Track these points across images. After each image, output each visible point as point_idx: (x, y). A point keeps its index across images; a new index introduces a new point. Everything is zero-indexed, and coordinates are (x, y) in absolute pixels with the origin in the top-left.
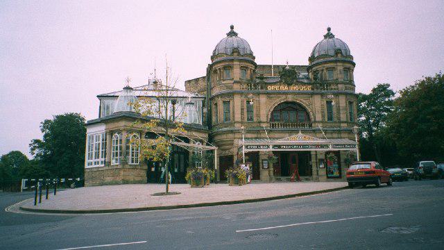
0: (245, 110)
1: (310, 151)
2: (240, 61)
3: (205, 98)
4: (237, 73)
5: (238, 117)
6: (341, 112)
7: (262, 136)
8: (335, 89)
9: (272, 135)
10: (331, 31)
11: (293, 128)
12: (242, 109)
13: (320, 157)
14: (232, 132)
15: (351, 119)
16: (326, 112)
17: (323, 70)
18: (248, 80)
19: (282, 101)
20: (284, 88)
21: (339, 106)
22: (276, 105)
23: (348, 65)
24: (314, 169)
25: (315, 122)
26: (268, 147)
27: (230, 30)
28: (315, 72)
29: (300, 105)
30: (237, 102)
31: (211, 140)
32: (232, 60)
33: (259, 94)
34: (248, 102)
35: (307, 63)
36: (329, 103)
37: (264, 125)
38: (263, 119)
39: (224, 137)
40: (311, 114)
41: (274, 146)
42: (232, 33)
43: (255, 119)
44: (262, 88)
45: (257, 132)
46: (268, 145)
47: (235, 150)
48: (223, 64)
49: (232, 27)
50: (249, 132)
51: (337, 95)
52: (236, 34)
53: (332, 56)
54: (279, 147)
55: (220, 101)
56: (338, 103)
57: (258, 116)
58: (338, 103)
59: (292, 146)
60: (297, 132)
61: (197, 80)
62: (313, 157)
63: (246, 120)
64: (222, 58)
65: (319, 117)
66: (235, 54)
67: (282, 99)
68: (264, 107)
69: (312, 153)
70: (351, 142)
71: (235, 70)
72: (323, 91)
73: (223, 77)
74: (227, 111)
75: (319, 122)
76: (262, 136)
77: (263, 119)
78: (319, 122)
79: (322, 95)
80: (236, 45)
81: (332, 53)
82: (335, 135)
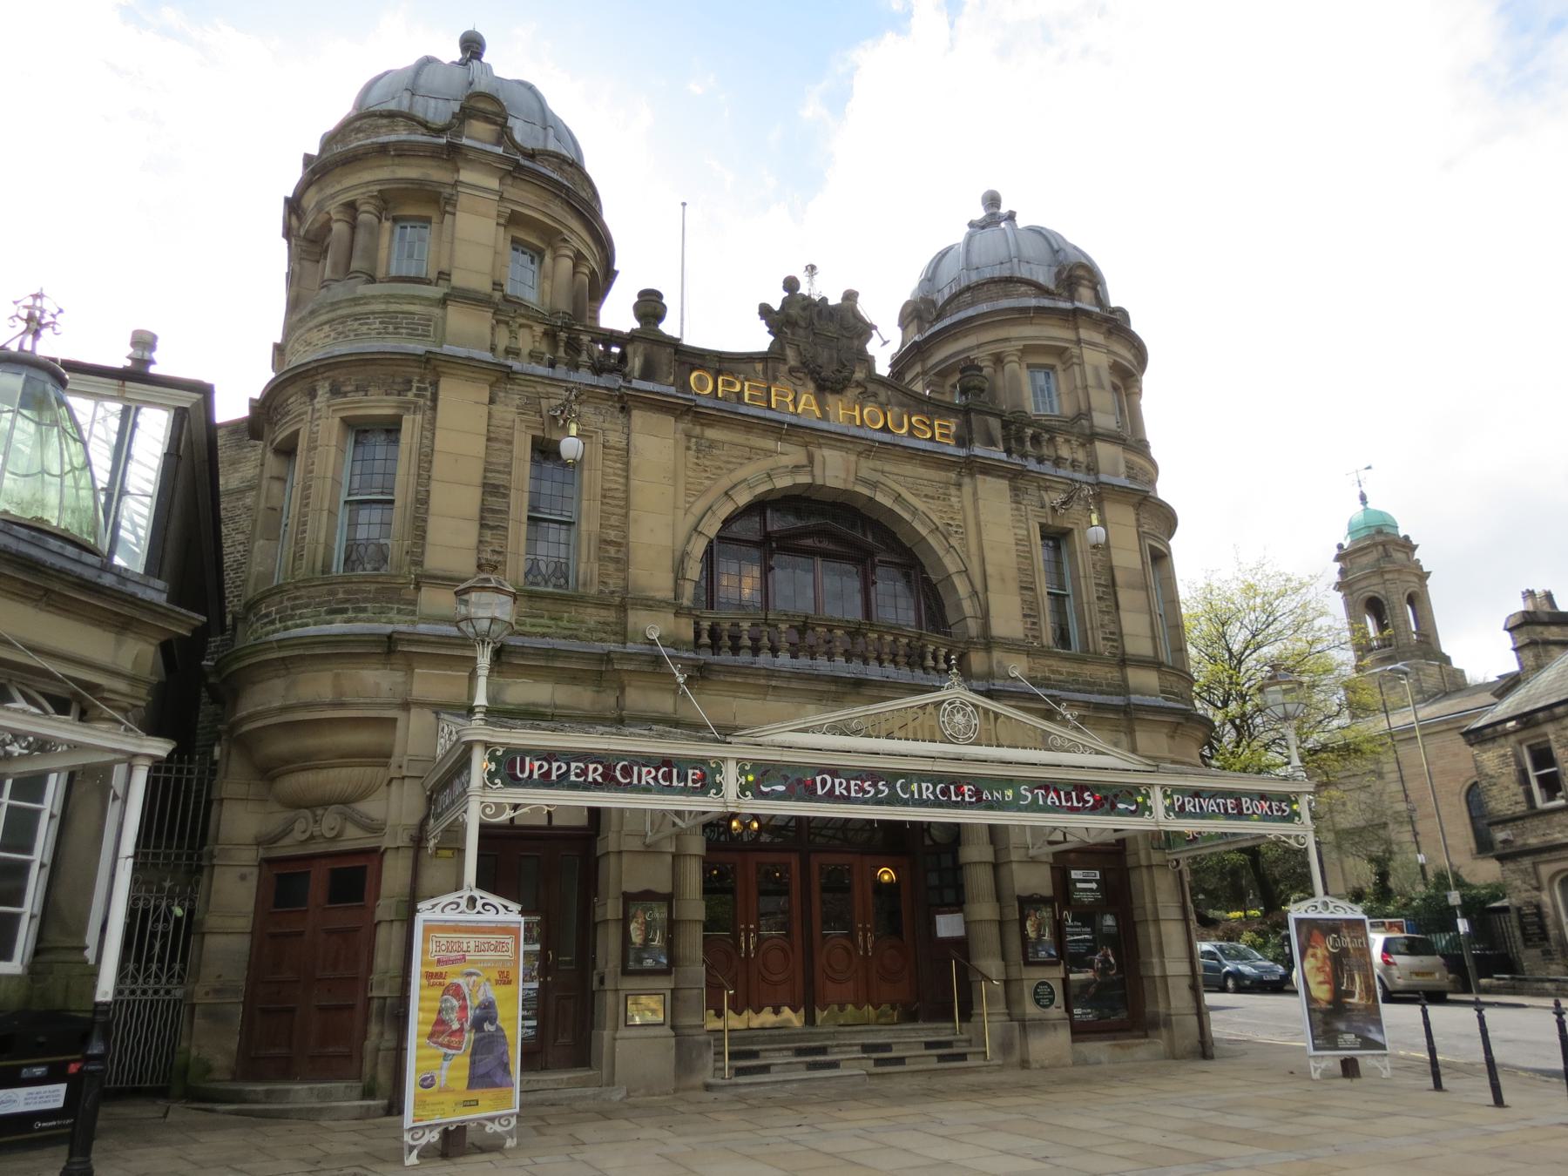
4: (474, 240)
6: (1124, 597)
8: (1074, 464)
10: (1004, 210)
11: (855, 669)
12: (492, 490)
16: (1043, 587)
17: (998, 360)
19: (783, 482)
21: (1111, 569)
22: (743, 498)
25: (988, 642)
26: (707, 784)
30: (462, 421)
33: (625, 404)
36: (1056, 538)
38: (652, 575)
39: (317, 686)
41: (761, 776)
44: (648, 373)
47: (397, 808)
48: (384, 173)
54: (801, 783)
57: (615, 551)
62: (979, 880)
67: (775, 468)
68: (663, 499)
73: (371, 254)
75: (1011, 646)
77: (652, 575)
78: (1011, 646)
79: (1016, 477)
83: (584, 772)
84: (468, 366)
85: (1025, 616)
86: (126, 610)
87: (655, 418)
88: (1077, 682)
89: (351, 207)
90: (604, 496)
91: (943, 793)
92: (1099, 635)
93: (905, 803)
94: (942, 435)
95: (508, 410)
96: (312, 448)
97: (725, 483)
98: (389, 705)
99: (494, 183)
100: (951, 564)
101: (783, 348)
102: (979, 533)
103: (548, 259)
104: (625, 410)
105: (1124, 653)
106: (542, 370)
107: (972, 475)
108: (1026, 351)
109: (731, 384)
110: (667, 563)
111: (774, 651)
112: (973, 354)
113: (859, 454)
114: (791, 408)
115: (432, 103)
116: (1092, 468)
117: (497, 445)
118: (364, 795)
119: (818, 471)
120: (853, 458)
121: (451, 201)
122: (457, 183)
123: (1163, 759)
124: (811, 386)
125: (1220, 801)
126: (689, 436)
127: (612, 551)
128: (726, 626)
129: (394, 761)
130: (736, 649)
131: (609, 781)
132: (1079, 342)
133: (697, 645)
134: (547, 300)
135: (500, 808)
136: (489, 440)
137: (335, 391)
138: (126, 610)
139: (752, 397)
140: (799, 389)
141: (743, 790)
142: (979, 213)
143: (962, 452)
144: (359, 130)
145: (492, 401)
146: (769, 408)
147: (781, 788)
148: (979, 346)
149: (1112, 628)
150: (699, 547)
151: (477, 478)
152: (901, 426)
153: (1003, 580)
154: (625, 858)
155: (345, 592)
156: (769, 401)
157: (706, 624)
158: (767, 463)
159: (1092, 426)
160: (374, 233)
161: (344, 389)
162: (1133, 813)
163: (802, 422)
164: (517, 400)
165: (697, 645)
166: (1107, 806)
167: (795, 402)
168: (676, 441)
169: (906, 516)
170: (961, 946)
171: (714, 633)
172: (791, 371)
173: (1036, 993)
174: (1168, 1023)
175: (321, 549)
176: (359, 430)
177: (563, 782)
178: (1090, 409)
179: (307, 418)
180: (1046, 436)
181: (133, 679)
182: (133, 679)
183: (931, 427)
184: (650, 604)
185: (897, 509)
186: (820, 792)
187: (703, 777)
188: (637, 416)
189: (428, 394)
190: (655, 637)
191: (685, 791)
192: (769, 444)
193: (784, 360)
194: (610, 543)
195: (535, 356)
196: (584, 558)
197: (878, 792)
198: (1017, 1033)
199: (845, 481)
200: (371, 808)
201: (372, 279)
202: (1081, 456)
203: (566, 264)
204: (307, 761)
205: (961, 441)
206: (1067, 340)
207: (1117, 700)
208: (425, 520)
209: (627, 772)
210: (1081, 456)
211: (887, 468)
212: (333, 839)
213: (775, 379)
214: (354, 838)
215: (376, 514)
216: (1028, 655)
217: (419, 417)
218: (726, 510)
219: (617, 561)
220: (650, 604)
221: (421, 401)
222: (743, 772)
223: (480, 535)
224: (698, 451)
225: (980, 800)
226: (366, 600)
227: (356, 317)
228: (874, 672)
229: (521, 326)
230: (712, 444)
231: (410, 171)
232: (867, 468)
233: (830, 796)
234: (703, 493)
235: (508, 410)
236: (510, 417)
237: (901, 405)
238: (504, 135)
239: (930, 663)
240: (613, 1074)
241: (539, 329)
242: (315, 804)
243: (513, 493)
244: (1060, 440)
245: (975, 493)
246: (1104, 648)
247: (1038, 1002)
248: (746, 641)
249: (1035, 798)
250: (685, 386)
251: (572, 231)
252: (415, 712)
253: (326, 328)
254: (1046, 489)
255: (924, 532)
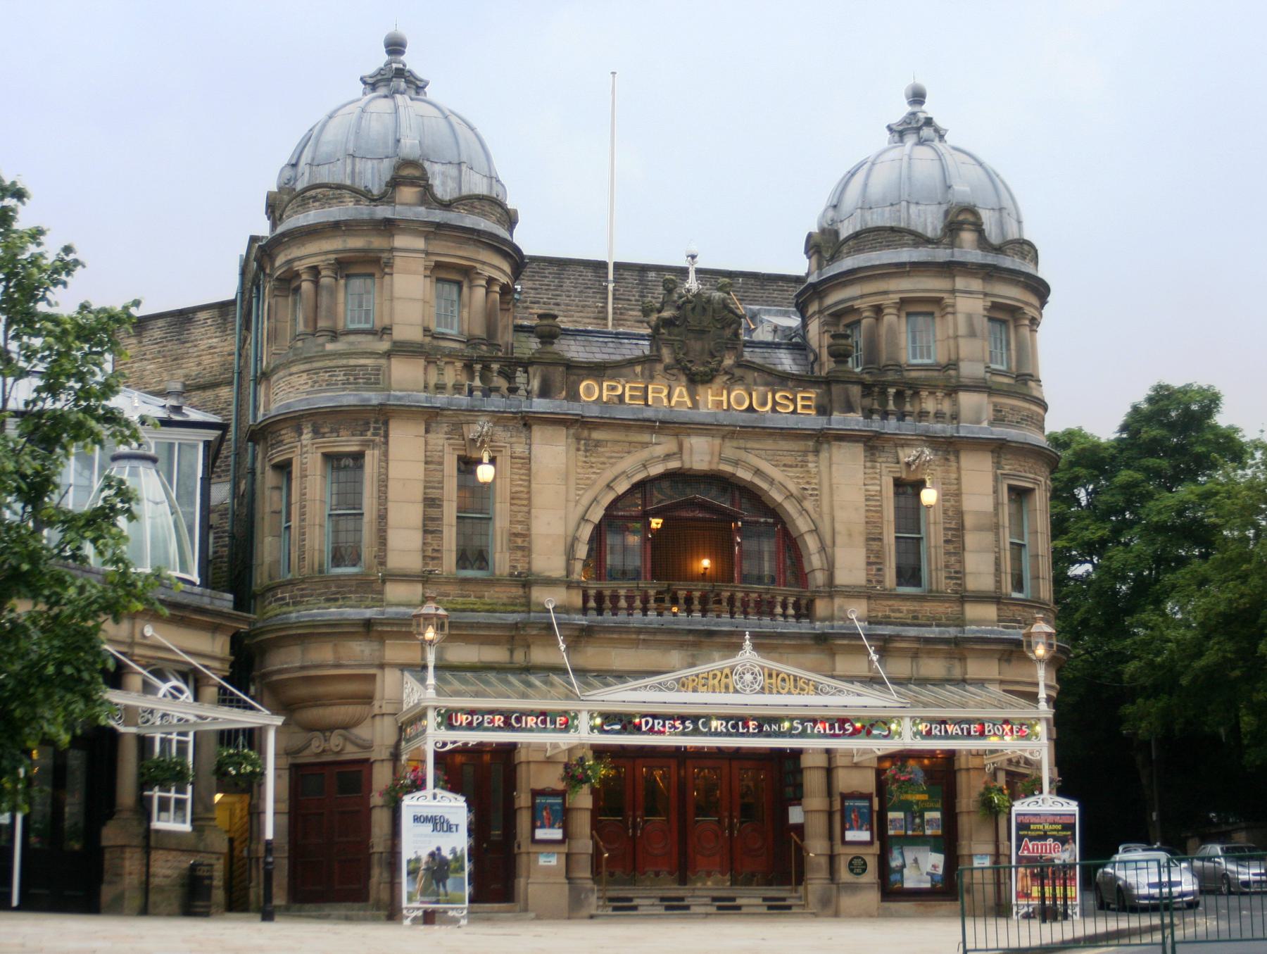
0: (450, 512)
1: (797, 754)
2: (436, 230)
3: (224, 427)
4: (409, 297)
5: (405, 546)
6: (970, 539)
7: (539, 656)
8: (939, 416)
9: (593, 656)
10: (929, 109)
12: (431, 502)
13: (846, 781)
14: (367, 628)
15: (1018, 585)
16: (890, 536)
17: (878, 310)
18: (471, 341)
20: (669, 396)
21: (960, 514)
22: (622, 487)
23: (1010, 293)
24: (816, 848)
25: (832, 590)
27: (380, 59)
28: (837, 316)
29: (751, 496)
30: (406, 458)
31: (246, 671)
32: (388, 226)
33: (527, 422)
34: (467, 465)
35: (798, 265)
36: (908, 488)
37: (550, 599)
38: (548, 561)
39: (323, 654)
40: (811, 543)
42: (394, 78)
43: (502, 561)
44: (545, 392)
45: (505, 629)
46: (568, 721)
47: (380, 734)
49: (395, 47)
50: (455, 630)
51: (950, 447)
52: (417, 86)
53: (928, 241)
55: (307, 454)
56: (952, 495)
57: (521, 542)
58: (952, 495)
59: (694, 721)
60: (732, 644)
61: (182, 319)
62: (813, 781)
63: (449, 562)
64: (334, 213)
65: (851, 566)
66: (408, 193)
67: (652, 457)
69: (806, 761)
70: (1019, 711)
71: (398, 278)
72: (876, 424)
73: (332, 313)
74: (347, 507)
75: (852, 593)
76: (539, 656)
77: (548, 561)
78: (852, 593)
79: (873, 443)
80: (410, 146)
81: (929, 220)
82: (934, 667)
83: (492, 721)
84: (408, 412)
85: (869, 564)
86: (218, 621)
87: (550, 431)
88: (915, 618)
89: (315, 271)
90: (512, 498)
91: (733, 727)
92: (943, 574)
93: (705, 734)
94: (804, 407)
95: (439, 439)
96: (304, 476)
97: (609, 474)
98: (371, 666)
99: (420, 243)
100: (802, 525)
101: (658, 350)
102: (831, 494)
103: (465, 289)
104: (527, 426)
105: (966, 591)
106: (463, 400)
107: (829, 443)
108: (904, 302)
109: (613, 388)
110: (561, 548)
111: (645, 611)
112: (857, 304)
113: (723, 437)
114: (665, 401)
115: (369, 163)
116: (955, 417)
117: (432, 467)
118: (357, 723)
119: (686, 457)
120: (717, 441)
121: (389, 264)
122: (392, 250)
123: (991, 681)
124: (684, 379)
125: (965, 726)
126: (578, 439)
127: (519, 541)
128: (607, 593)
129: (376, 703)
130: (615, 610)
131: (508, 726)
132: (953, 291)
133: (585, 610)
134: (466, 327)
135: (445, 744)
136: (426, 463)
137: (316, 432)
138: (218, 621)
139: (632, 397)
140: (673, 383)
141: (592, 728)
142: (900, 110)
143: (819, 422)
144: (315, 199)
145: (427, 431)
146: (647, 404)
147: (618, 727)
148: (862, 296)
149: (957, 567)
150: (586, 532)
151: (420, 497)
152: (764, 404)
153: (850, 535)
154: (532, 766)
155: (338, 587)
156: (646, 399)
157: (592, 592)
158: (644, 454)
159: (958, 376)
160: (333, 292)
161: (323, 430)
162: (885, 737)
163: (668, 418)
164: (445, 428)
165: (585, 610)
166: (864, 732)
167: (669, 397)
168: (568, 446)
169: (765, 486)
170: (799, 829)
171: (600, 598)
172: (667, 368)
173: (851, 863)
174: (969, 890)
175: (317, 554)
176: (331, 459)
177: (480, 727)
178: (958, 359)
179: (298, 450)
180: (909, 392)
181: (222, 660)
182: (222, 660)
183: (794, 401)
184: (549, 582)
185: (758, 481)
186: (644, 729)
187: (567, 722)
188: (537, 432)
189: (382, 432)
190: (551, 607)
191: (555, 730)
192: (645, 437)
193: (659, 359)
194: (516, 535)
195: (458, 388)
196: (499, 549)
197: (685, 728)
198: (834, 892)
199: (710, 462)
200: (362, 732)
201: (334, 335)
202: (946, 406)
203: (480, 293)
204: (317, 701)
205: (823, 410)
206: (941, 291)
207: (952, 632)
208: (385, 531)
209: (518, 720)
210: (946, 406)
211: (750, 445)
212: (338, 753)
213: (652, 377)
214: (351, 753)
215: (351, 524)
216: (869, 598)
217: (376, 452)
218: (610, 497)
219: (522, 548)
220: (549, 582)
221: (377, 439)
222: (592, 717)
223: (424, 538)
224: (586, 451)
225: (761, 731)
226: (351, 592)
227: (326, 369)
228: (724, 622)
229: (446, 363)
230: (598, 443)
231: (356, 243)
232: (730, 450)
233: (651, 731)
234: (590, 486)
235: (439, 439)
236: (441, 442)
237: (766, 384)
238: (428, 197)
239: (779, 610)
240: (527, 904)
241: (459, 365)
242: (326, 729)
243: (445, 504)
244: (924, 394)
245: (830, 458)
246: (943, 583)
247: (852, 870)
248: (623, 603)
249: (805, 729)
250: (574, 396)
251: (484, 263)
252: (388, 672)
253: (305, 375)
254: (902, 446)
255: (778, 497)
